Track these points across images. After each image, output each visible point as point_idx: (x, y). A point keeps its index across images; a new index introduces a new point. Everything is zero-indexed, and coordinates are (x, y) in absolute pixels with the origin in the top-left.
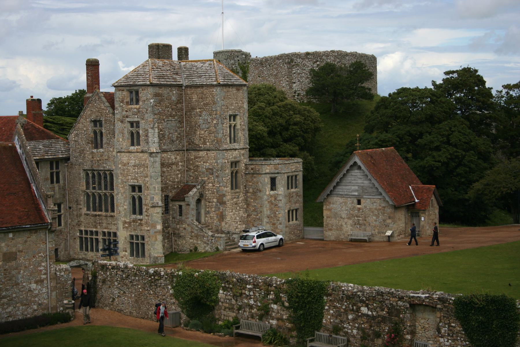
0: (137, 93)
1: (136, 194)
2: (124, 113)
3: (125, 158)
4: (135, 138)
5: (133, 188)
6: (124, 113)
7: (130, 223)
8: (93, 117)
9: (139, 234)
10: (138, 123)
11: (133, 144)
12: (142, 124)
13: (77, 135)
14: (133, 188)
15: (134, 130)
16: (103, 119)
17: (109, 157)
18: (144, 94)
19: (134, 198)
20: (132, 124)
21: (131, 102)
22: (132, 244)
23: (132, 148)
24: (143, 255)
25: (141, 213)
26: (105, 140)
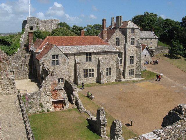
0: (133, 30)
1: (132, 58)
2: (130, 36)
3: (129, 49)
4: (132, 43)
5: (131, 57)
6: (130, 36)
7: (130, 66)
8: (117, 37)
9: (132, 69)
10: (133, 39)
11: (131, 44)
12: (135, 39)
13: (111, 42)
14: (131, 57)
15: (132, 40)
16: (120, 37)
17: (121, 48)
18: (136, 30)
19: (131, 59)
20: (131, 39)
21: (132, 32)
22: (130, 72)
23: (132, 46)
24: (133, 74)
25: (133, 63)
26: (120, 44)
